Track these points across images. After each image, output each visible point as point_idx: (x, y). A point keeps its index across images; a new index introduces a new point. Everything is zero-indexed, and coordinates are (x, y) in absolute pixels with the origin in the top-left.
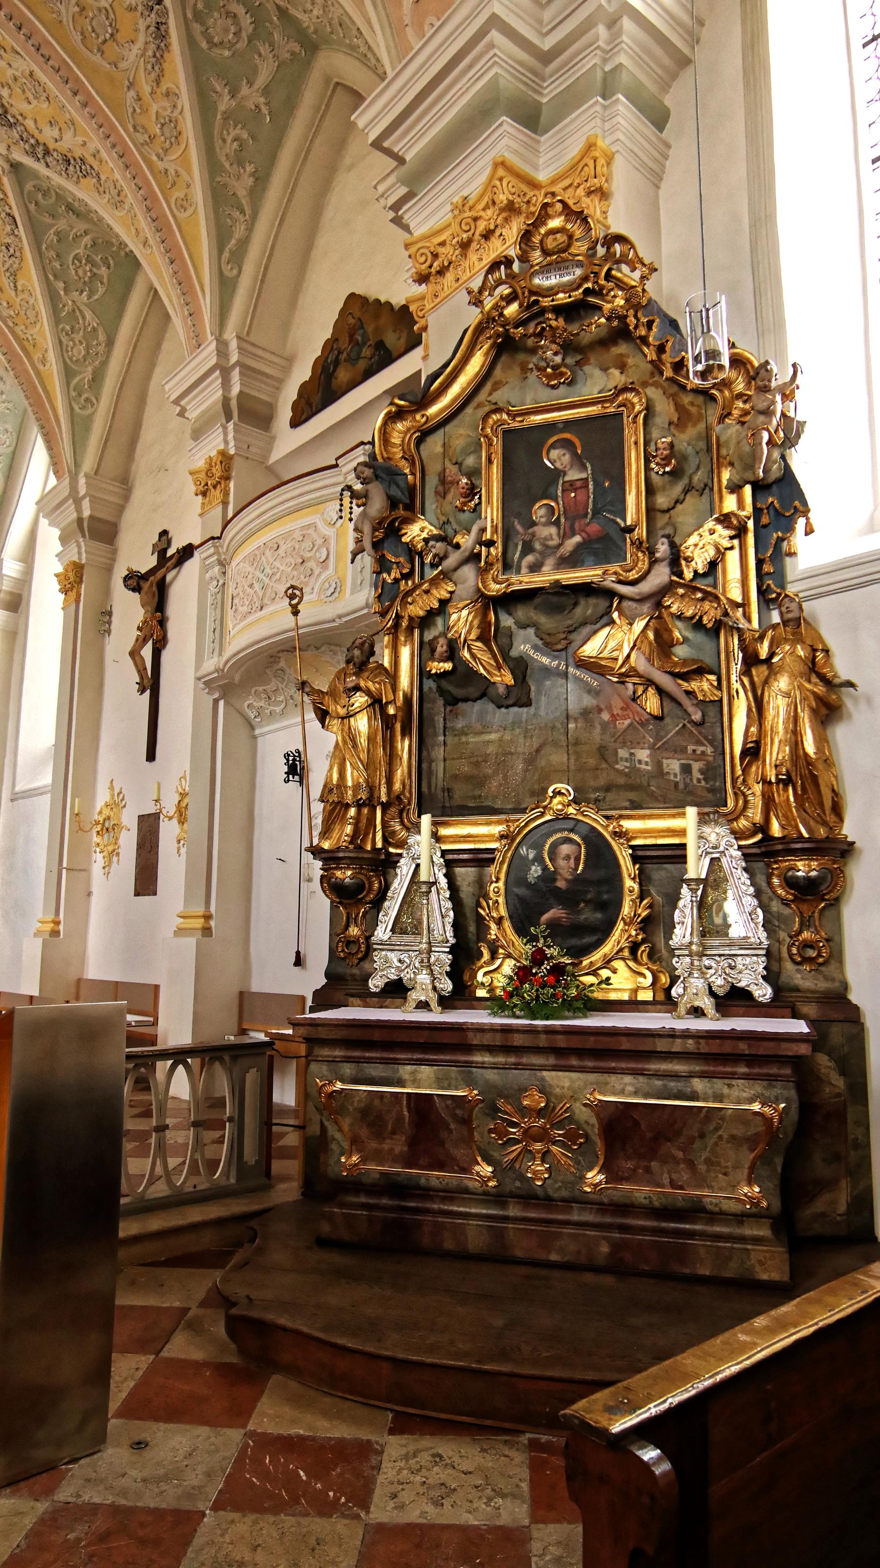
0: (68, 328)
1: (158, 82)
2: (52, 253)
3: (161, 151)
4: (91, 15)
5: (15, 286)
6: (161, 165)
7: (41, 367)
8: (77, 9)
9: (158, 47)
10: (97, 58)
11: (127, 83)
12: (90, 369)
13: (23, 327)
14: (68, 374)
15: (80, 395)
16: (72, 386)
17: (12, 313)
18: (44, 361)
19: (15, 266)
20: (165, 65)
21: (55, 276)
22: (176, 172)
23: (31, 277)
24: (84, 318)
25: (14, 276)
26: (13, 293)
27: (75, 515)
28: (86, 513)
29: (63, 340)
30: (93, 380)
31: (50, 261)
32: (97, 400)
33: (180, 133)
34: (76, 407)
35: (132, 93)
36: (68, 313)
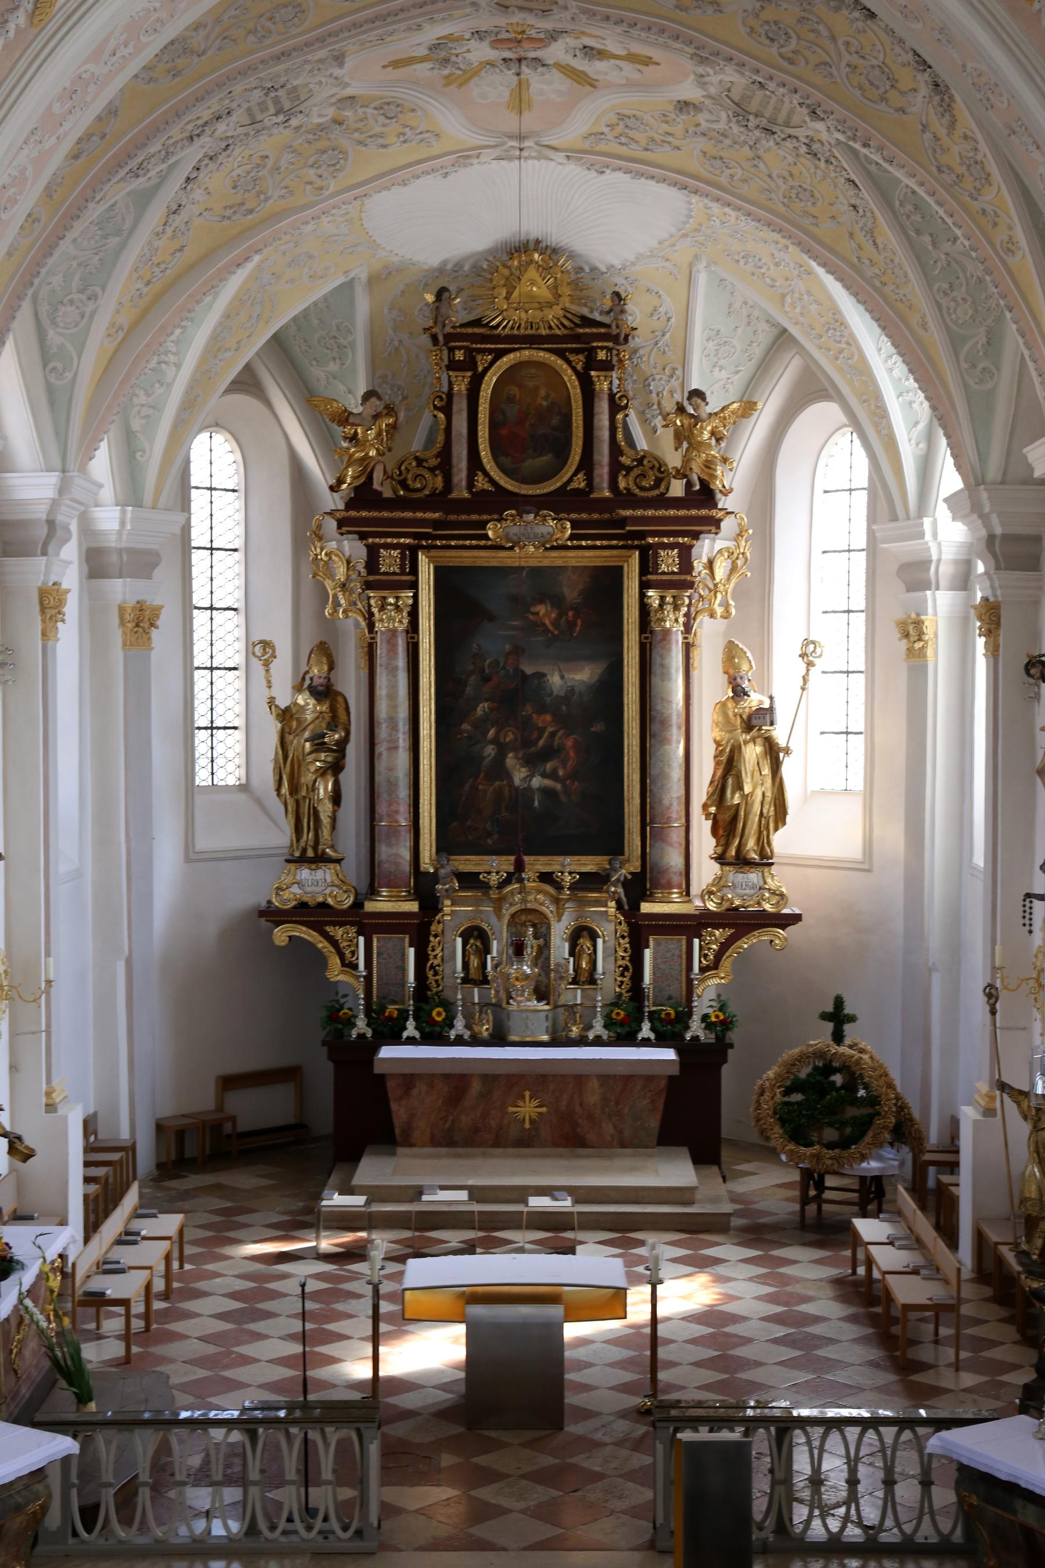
0: (945, 286)
1: (952, 125)
2: (909, 207)
3: (973, 191)
4: (865, 72)
5: (875, 244)
6: (975, 205)
7: (922, 332)
8: (848, 69)
9: (942, 100)
10: (883, 106)
11: (920, 127)
12: (982, 330)
13: (893, 287)
14: (955, 343)
15: (974, 366)
16: (962, 356)
17: (878, 272)
18: (924, 326)
19: (870, 224)
20: (955, 112)
21: (918, 232)
22: (995, 212)
23: (888, 235)
24: (964, 270)
25: (871, 233)
26: (874, 251)
27: (984, 533)
28: (998, 531)
29: (944, 302)
30: (988, 343)
31: (908, 217)
32: (998, 369)
33: (989, 175)
34: (971, 382)
35: (928, 136)
36: (943, 268)
